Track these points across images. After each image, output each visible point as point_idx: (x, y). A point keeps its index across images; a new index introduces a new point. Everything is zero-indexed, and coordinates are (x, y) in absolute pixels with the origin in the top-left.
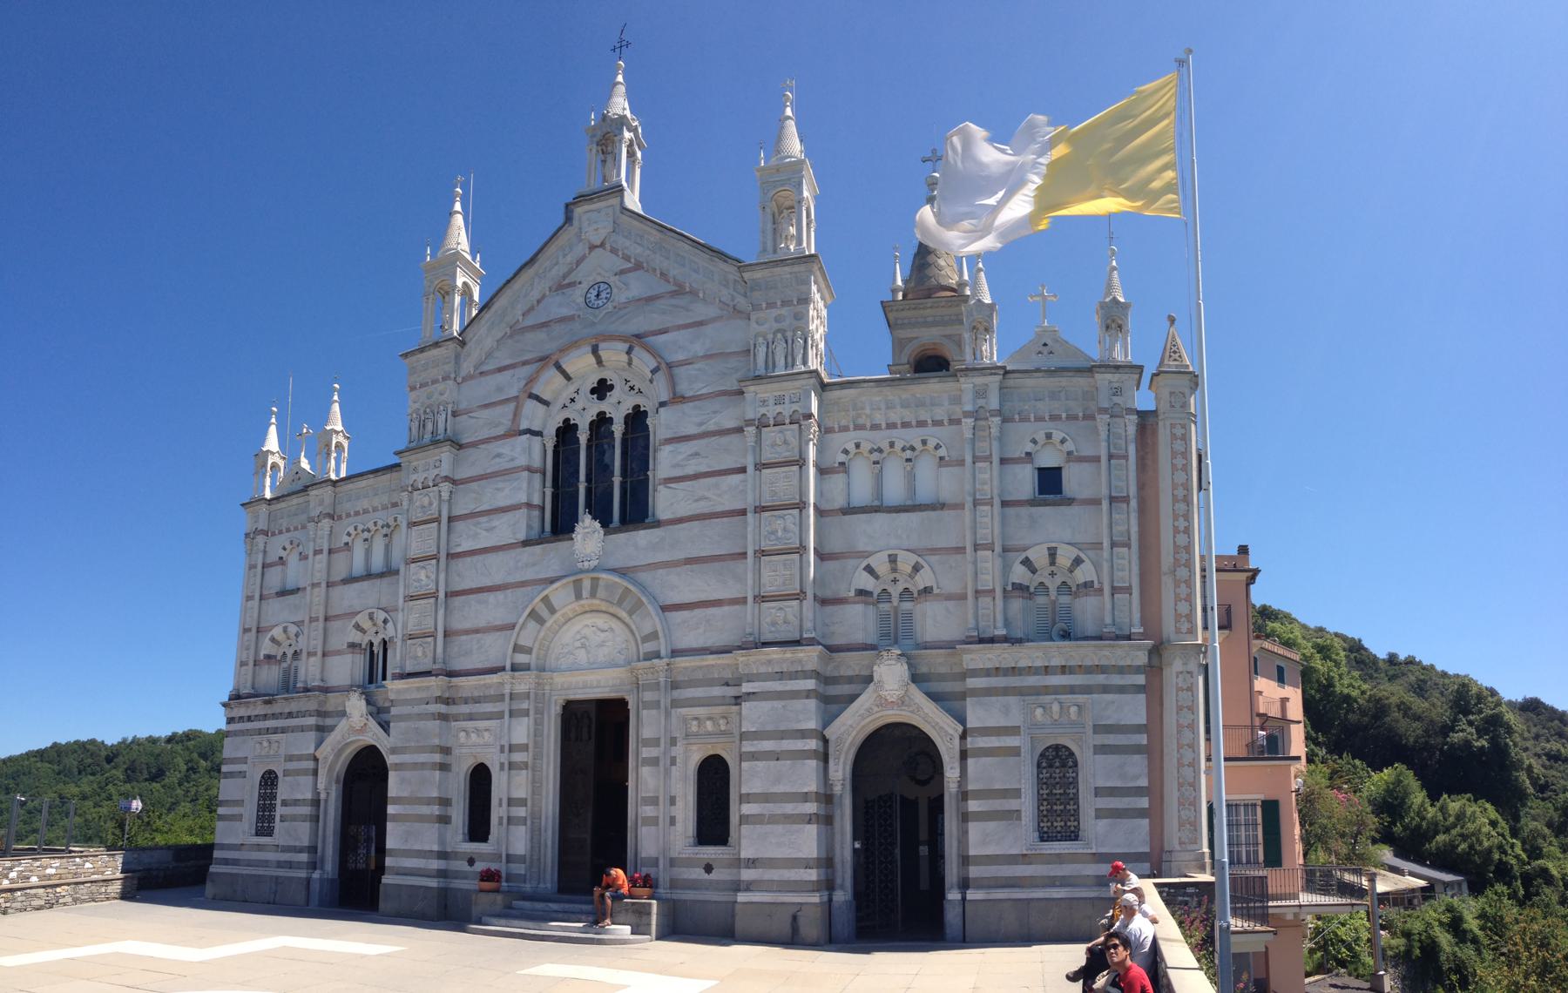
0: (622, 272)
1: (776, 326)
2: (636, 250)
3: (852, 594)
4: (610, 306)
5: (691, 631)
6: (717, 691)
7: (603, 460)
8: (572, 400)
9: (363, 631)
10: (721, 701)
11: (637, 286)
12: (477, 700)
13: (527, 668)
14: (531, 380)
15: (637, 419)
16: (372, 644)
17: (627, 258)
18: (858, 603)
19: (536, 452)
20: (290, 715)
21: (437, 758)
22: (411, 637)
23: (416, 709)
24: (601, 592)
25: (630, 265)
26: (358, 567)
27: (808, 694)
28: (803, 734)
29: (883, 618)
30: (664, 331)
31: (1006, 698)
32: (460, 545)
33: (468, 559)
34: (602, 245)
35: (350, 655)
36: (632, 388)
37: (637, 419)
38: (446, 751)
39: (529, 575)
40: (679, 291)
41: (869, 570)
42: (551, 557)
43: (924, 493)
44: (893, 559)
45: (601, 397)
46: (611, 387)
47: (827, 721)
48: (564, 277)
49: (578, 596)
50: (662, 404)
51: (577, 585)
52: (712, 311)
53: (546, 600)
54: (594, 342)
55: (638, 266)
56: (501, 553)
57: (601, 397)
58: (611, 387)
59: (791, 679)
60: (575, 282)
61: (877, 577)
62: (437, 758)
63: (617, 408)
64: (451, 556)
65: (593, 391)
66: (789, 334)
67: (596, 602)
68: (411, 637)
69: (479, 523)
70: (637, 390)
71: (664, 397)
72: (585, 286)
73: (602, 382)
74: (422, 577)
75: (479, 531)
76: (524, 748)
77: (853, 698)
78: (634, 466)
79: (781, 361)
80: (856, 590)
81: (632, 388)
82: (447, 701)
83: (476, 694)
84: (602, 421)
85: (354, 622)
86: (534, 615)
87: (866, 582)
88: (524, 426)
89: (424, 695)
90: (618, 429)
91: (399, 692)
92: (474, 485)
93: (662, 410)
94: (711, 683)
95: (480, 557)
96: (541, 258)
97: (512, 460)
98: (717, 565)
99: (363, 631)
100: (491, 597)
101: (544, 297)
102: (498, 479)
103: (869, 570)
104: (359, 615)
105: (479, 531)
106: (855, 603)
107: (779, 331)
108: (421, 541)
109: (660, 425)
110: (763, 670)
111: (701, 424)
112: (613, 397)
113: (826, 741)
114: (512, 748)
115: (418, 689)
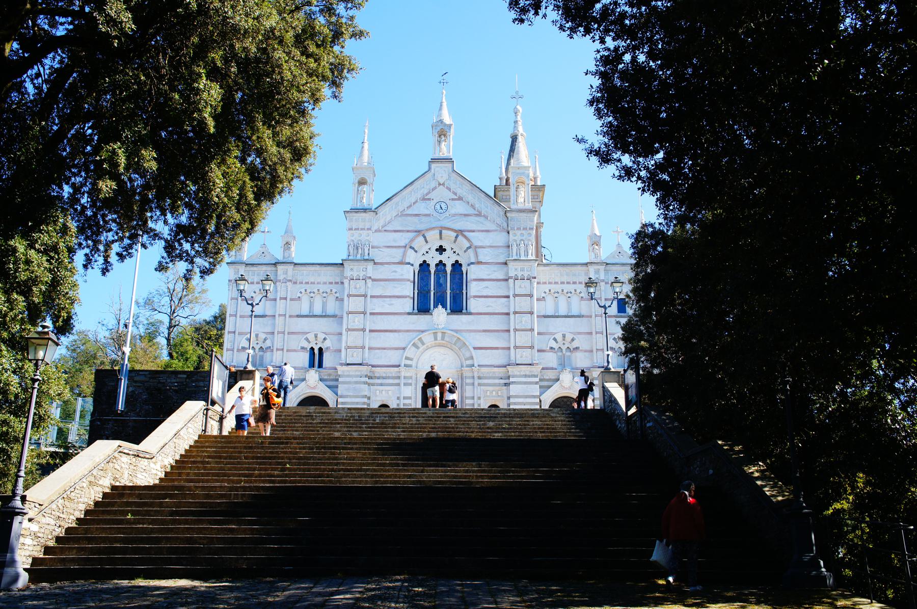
0: (453, 199)
1: (521, 238)
2: (460, 192)
3: (548, 348)
4: (447, 214)
5: (481, 358)
6: (497, 381)
8: (427, 252)
9: (309, 342)
10: (499, 385)
11: (459, 208)
12: (384, 378)
13: (410, 366)
14: (412, 240)
15: (457, 265)
16: (312, 349)
17: (456, 194)
19: (409, 272)
21: (366, 400)
22: (349, 347)
23: (355, 379)
24: (447, 339)
25: (456, 197)
26: (305, 310)
27: (536, 383)
28: (534, 397)
29: (559, 358)
30: (473, 231)
33: (379, 316)
34: (443, 184)
36: (454, 252)
37: (457, 265)
38: (369, 398)
39: (411, 327)
40: (479, 215)
41: (555, 340)
42: (422, 321)
43: (575, 312)
44: (564, 336)
45: (441, 254)
46: (445, 250)
47: (541, 394)
48: (427, 194)
49: (436, 339)
50: (472, 263)
51: (435, 334)
52: (492, 227)
53: (420, 339)
54: (440, 229)
55: (460, 199)
57: (441, 254)
58: (445, 250)
61: (557, 342)
62: (366, 400)
63: (448, 259)
64: (364, 313)
65: (437, 250)
66: (526, 242)
67: (443, 342)
68: (349, 347)
72: (435, 201)
73: (441, 246)
74: (357, 321)
76: (410, 398)
77: (549, 387)
79: (522, 253)
81: (454, 252)
82: (370, 378)
83: (384, 375)
85: (305, 337)
86: (414, 345)
87: (554, 345)
88: (407, 261)
89: (359, 373)
90: (449, 269)
91: (343, 371)
92: (382, 283)
93: (472, 266)
94: (494, 378)
96: (416, 184)
97: (402, 275)
98: (496, 333)
99: (309, 342)
100: (391, 334)
101: (416, 202)
103: (555, 340)
104: (424, 334)
107: (522, 240)
108: (355, 304)
109: (472, 272)
110: (518, 374)
111: (489, 275)
113: (540, 401)
114: (405, 398)
115: (356, 371)
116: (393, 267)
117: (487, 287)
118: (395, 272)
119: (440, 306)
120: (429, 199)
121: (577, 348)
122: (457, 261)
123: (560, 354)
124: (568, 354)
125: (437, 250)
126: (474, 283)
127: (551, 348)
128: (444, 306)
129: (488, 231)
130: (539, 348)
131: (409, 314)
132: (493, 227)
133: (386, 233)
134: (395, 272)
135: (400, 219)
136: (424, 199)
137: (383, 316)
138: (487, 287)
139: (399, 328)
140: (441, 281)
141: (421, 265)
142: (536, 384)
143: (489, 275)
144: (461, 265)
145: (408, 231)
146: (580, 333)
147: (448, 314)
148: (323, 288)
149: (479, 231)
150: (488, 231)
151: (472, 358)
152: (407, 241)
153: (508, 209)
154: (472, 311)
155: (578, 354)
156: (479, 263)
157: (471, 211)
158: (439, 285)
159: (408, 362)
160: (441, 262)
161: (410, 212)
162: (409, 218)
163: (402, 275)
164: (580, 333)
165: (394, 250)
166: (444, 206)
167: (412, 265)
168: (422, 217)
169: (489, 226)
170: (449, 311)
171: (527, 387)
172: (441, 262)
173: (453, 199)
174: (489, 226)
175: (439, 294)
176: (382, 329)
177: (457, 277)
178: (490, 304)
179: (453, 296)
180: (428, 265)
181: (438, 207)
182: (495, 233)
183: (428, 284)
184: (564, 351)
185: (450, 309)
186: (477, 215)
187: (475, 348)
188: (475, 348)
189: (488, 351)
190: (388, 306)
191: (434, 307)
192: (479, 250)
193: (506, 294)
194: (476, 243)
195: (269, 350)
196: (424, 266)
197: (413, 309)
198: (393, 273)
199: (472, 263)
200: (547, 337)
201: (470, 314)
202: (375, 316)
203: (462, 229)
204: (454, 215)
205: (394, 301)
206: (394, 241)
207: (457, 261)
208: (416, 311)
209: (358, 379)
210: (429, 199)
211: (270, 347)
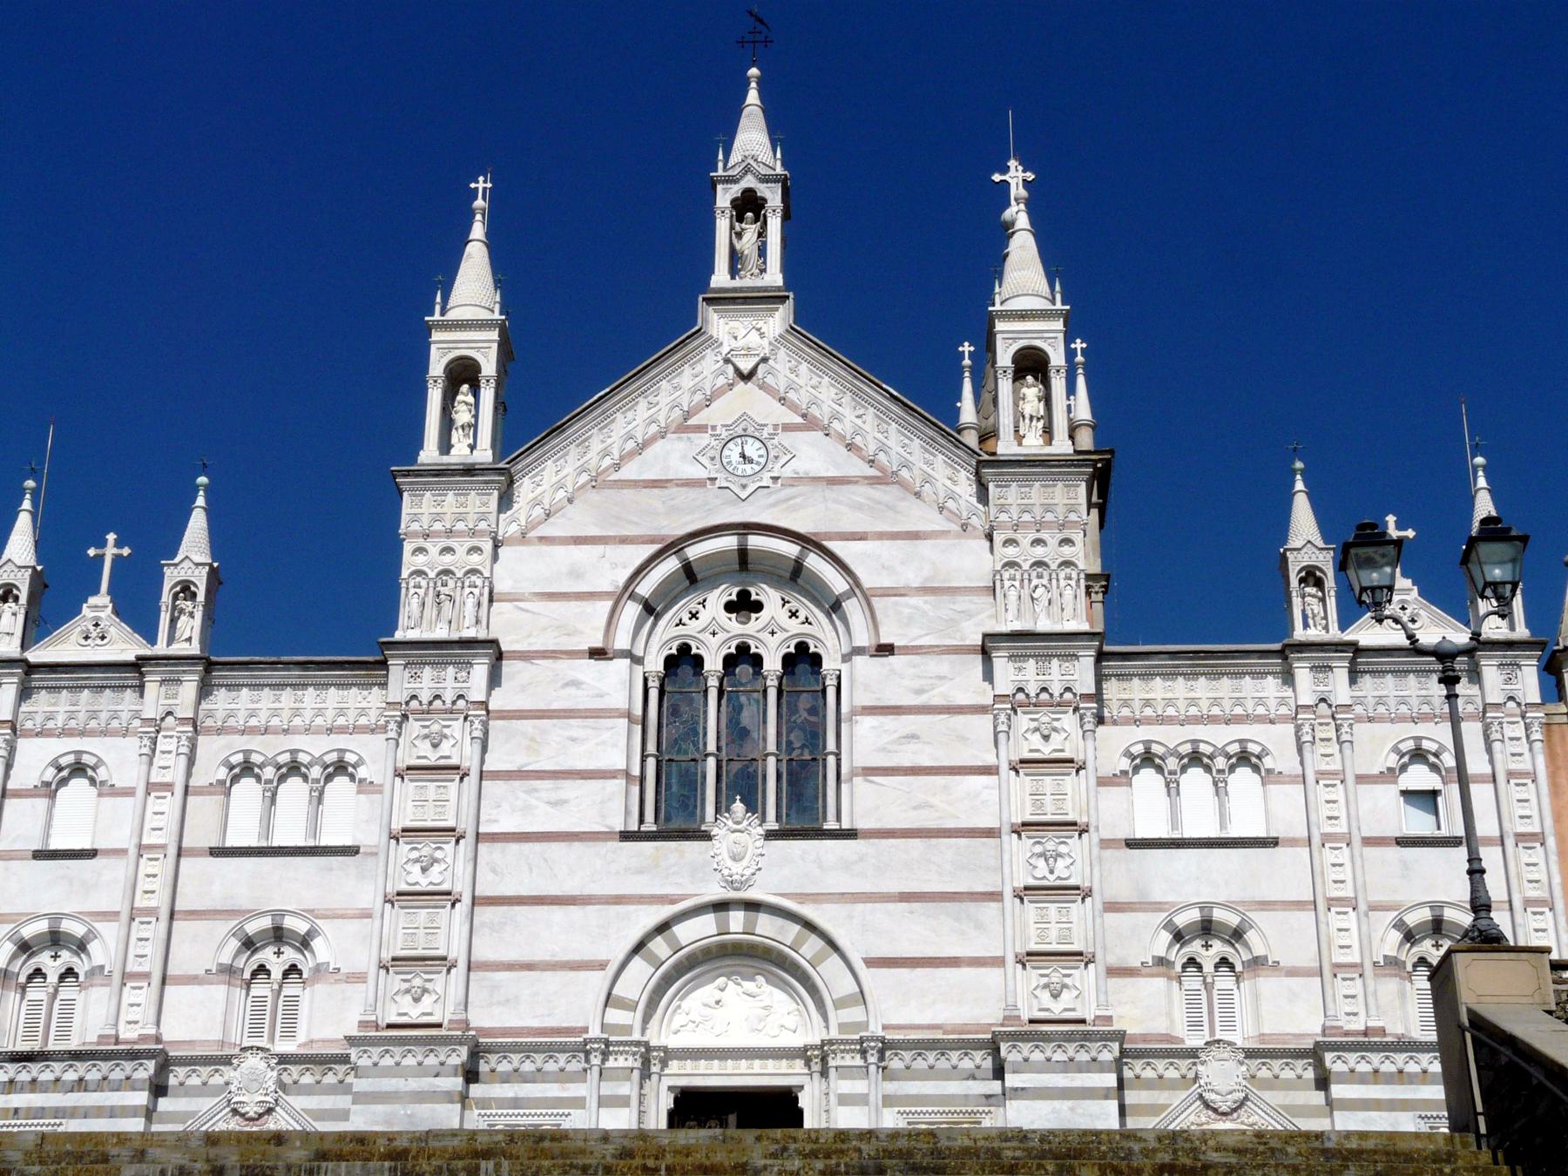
0: (788, 428)
7: (738, 723)
8: (694, 616)
15: (802, 659)
17: (793, 407)
18: (1158, 975)
20: (81, 1085)
23: (414, 1084)
30: (861, 537)
31: (1394, 1113)
32: (496, 821)
33: (514, 847)
35: (223, 988)
36: (794, 614)
37: (802, 659)
40: (885, 478)
46: (758, 607)
50: (858, 651)
55: (809, 423)
56: (577, 844)
58: (758, 607)
59: (1080, 1072)
60: (706, 426)
65: (730, 607)
69: (536, 790)
70: (802, 618)
71: (863, 638)
73: (743, 595)
75: (533, 802)
78: (792, 737)
80: (1153, 957)
84: (743, 657)
93: (858, 659)
95: (537, 847)
97: (601, 696)
100: (557, 913)
102: (572, 721)
105: (533, 802)
106: (1152, 976)
111: (919, 692)
112: (756, 623)
116: (565, 667)
117: (913, 737)
118: (575, 683)
119: (738, 807)
120: (701, 429)
121: (1257, 963)
122: (802, 647)
123: (1193, 982)
124: (1225, 982)
125: (730, 607)
126: (866, 724)
127: (1161, 961)
128: (753, 805)
129: (915, 536)
130: (1112, 960)
131: (626, 836)
132: (937, 522)
133: (545, 548)
134: (575, 683)
135: (594, 496)
136: (684, 426)
137: (527, 847)
138: (913, 737)
139: (586, 892)
140: (746, 718)
141: (670, 662)
142: (1106, 1097)
143: (919, 692)
144: (816, 660)
145: (624, 540)
146: (1265, 905)
147: (770, 835)
148: (315, 747)
149: (881, 536)
150: (915, 536)
151: (861, 997)
152: (623, 576)
153: (986, 457)
154: (861, 824)
155: (1267, 984)
156: (886, 650)
157: (860, 468)
158: (737, 732)
159: (616, 1016)
160: (743, 649)
161: (630, 471)
162: (628, 493)
163: (601, 696)
164: (1265, 905)
165: (574, 607)
166: (752, 449)
167: (637, 660)
168: (674, 490)
169: (921, 517)
170: (772, 824)
171: (1072, 1109)
172: (743, 649)
173: (788, 428)
174: (921, 517)
175: (736, 766)
176: (524, 892)
177: (804, 702)
178: (934, 801)
179: (790, 774)
180: (698, 661)
181: (733, 452)
182: (942, 542)
183: (694, 732)
184: (1208, 967)
185: (778, 818)
186: (874, 481)
187: (872, 962)
188: (872, 962)
189: (920, 971)
190: (549, 809)
191: (718, 811)
192: (875, 601)
193: (990, 759)
194: (867, 581)
195: (98, 979)
196: (683, 660)
197: (641, 821)
198: (572, 691)
199: (858, 651)
200: (1140, 917)
201: (851, 834)
202: (499, 846)
203: (822, 528)
204: (797, 480)
205: (571, 789)
206: (575, 573)
207: (802, 647)
208: (649, 825)
209: (427, 1083)
210: (701, 429)
211: (102, 967)
